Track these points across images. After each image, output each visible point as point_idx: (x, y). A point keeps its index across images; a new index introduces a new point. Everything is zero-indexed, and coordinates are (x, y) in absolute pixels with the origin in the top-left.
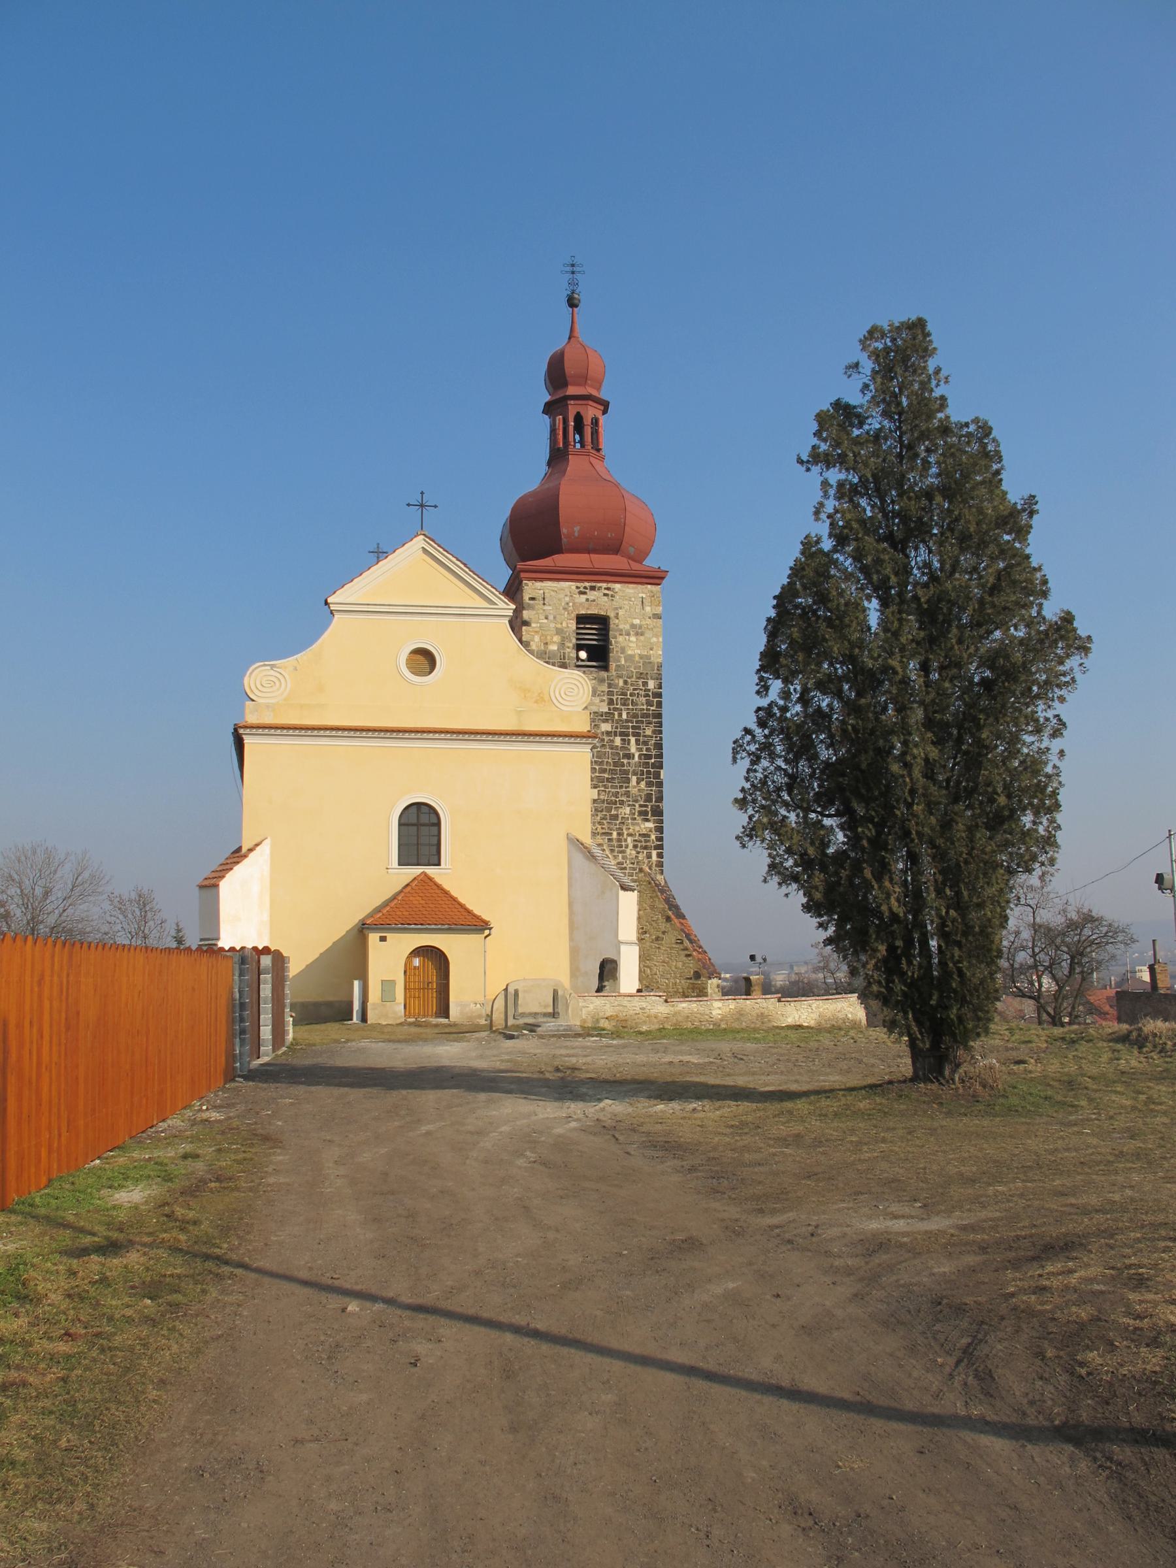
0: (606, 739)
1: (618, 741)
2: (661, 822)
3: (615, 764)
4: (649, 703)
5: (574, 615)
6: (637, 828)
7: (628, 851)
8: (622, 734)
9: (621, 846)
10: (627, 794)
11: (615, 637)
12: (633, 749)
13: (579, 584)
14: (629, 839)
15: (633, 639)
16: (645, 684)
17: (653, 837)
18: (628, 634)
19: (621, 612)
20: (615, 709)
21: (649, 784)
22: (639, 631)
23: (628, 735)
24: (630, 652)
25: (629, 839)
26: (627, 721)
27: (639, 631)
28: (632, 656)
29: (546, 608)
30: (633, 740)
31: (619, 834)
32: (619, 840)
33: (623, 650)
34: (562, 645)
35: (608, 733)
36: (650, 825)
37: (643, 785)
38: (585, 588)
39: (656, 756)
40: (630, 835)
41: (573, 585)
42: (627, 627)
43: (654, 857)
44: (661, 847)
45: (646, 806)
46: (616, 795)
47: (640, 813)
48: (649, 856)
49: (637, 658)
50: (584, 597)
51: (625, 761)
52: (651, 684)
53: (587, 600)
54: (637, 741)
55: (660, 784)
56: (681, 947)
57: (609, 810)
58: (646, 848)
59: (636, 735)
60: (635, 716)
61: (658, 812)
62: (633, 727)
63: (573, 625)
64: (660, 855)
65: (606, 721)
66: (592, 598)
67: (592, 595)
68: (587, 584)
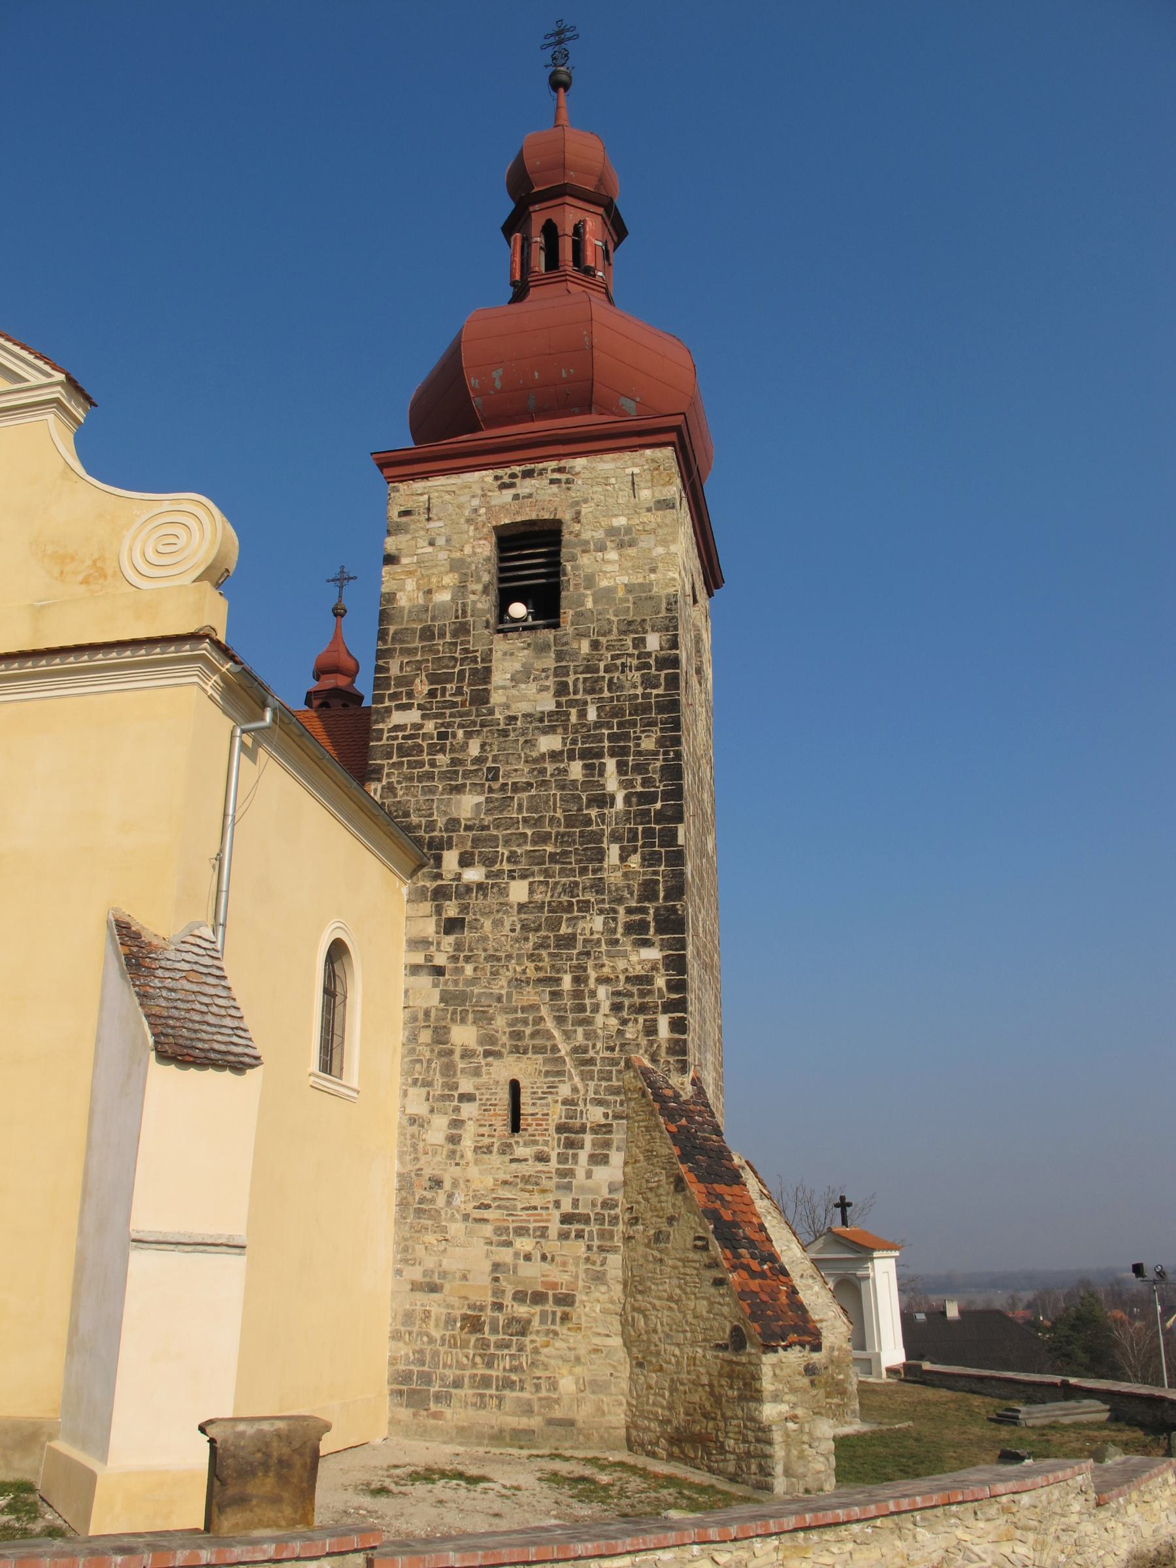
0: (550, 767)
1: (576, 770)
2: (682, 944)
3: (570, 821)
4: (648, 682)
6: (621, 964)
7: (599, 1020)
8: (585, 754)
9: (582, 1008)
10: (598, 886)
11: (573, 558)
12: (612, 783)
13: (500, 472)
14: (602, 992)
15: (612, 555)
16: (640, 642)
17: (660, 982)
18: (602, 548)
19: (585, 509)
20: (571, 704)
21: (650, 860)
22: (623, 539)
23: (600, 755)
24: (604, 583)
26: (598, 725)
27: (623, 539)
28: (610, 591)
29: (432, 525)
30: (611, 764)
31: (577, 980)
32: (577, 994)
33: (590, 581)
34: (461, 589)
35: (554, 756)
36: (653, 954)
37: (635, 861)
39: (667, 795)
40: (606, 980)
41: (488, 476)
42: (600, 534)
44: (680, 1005)
45: (644, 910)
46: (572, 889)
47: (629, 928)
48: (651, 1030)
49: (621, 593)
50: (508, 494)
51: (593, 812)
52: (653, 642)
53: (516, 497)
54: (621, 768)
55: (677, 858)
56: (702, 1257)
57: (554, 925)
58: (642, 1009)
59: (619, 752)
60: (617, 712)
61: (673, 924)
62: (612, 737)
63: (486, 549)
64: (678, 1026)
65: (551, 730)
66: (527, 491)
67: (525, 487)
68: (517, 469)
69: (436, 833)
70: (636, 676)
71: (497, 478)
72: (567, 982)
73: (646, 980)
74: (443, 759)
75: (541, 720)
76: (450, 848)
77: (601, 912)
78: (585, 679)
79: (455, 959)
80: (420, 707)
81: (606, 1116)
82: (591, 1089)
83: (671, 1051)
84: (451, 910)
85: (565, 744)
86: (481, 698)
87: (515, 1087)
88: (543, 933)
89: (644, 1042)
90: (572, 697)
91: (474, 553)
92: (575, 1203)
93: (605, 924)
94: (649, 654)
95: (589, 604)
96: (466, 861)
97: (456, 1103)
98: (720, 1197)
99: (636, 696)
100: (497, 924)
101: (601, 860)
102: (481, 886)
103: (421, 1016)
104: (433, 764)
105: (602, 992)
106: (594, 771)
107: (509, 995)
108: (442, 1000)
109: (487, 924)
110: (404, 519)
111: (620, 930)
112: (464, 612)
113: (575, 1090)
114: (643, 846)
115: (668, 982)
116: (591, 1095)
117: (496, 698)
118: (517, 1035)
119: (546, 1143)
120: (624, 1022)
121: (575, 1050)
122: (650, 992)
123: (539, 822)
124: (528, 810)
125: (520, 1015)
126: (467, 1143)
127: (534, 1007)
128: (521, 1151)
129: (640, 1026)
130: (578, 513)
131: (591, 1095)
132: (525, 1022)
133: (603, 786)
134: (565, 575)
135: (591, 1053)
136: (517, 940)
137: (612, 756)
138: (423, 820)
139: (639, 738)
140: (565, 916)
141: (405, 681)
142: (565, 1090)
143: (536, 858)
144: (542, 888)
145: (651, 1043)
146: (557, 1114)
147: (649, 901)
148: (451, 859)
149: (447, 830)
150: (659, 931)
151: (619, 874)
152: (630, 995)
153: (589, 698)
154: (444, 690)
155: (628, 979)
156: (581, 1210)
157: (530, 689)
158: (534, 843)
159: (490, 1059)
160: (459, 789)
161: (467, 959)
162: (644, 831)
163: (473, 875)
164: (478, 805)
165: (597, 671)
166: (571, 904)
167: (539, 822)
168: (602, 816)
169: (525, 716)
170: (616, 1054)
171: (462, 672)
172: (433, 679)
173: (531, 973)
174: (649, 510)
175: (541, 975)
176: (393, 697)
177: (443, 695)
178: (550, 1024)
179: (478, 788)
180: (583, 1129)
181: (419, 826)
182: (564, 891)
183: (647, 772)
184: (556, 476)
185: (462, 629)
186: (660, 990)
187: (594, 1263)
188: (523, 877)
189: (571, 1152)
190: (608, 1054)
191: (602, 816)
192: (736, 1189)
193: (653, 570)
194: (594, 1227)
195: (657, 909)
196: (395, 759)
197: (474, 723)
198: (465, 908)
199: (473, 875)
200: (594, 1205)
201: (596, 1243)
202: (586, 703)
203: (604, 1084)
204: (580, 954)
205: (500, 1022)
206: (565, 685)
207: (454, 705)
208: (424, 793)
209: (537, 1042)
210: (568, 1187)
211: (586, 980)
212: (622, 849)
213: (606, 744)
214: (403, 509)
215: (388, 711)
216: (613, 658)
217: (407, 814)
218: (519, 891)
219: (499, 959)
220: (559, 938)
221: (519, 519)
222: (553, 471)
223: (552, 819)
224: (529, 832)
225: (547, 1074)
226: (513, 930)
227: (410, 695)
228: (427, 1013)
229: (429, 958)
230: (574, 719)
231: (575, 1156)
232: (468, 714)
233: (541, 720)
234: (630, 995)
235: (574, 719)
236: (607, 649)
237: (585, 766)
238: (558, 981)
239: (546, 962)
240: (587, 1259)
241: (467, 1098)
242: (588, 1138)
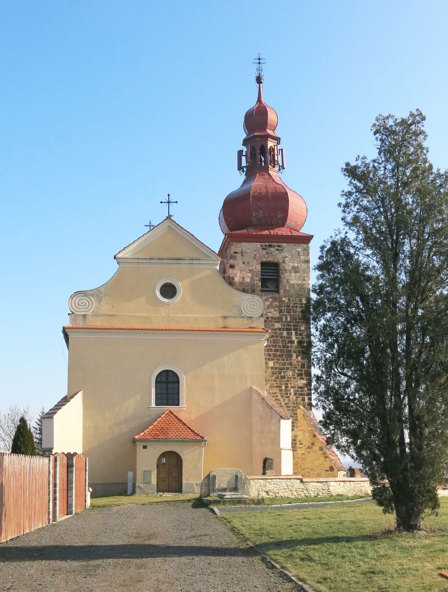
1: (285, 333)
3: (284, 347)
5: (259, 262)
7: (291, 397)
8: (287, 329)
9: (287, 394)
10: (291, 364)
13: (262, 244)
14: (292, 390)
15: (293, 274)
16: (301, 300)
20: (283, 315)
24: (292, 282)
25: (292, 390)
26: (290, 322)
28: (293, 285)
30: (293, 333)
31: (286, 387)
32: (286, 390)
33: (287, 281)
34: (252, 278)
35: (279, 329)
37: (300, 358)
38: (266, 246)
40: (293, 387)
41: (258, 245)
43: (307, 400)
45: (302, 371)
48: (303, 400)
49: (296, 286)
50: (265, 251)
51: (289, 345)
53: (267, 253)
54: (296, 334)
56: (322, 452)
57: (280, 373)
58: (301, 395)
59: (296, 330)
60: (295, 319)
62: (294, 325)
63: (259, 267)
65: (278, 322)
68: (267, 244)
71: (261, 246)
72: (283, 387)
77: (291, 370)
78: (287, 309)
88: (277, 375)
89: (302, 402)
93: (293, 373)
95: (288, 288)
101: (291, 357)
105: (292, 390)
106: (289, 334)
107: (269, 390)
110: (235, 254)
111: (296, 375)
112: (254, 285)
120: (297, 397)
121: (286, 404)
122: (303, 391)
123: (276, 346)
124: (273, 343)
129: (301, 399)
130: (284, 261)
134: (281, 278)
135: (289, 405)
136: (271, 376)
137: (294, 330)
140: (283, 371)
143: (275, 356)
144: (277, 364)
145: (304, 403)
151: (296, 361)
152: (298, 391)
155: (298, 387)
157: (272, 310)
158: (274, 352)
166: (284, 368)
167: (276, 346)
168: (291, 346)
169: (271, 317)
170: (295, 405)
173: (275, 385)
174: (303, 263)
175: (277, 385)
178: (279, 397)
182: (282, 365)
184: (278, 248)
188: (272, 360)
190: (293, 405)
191: (291, 346)
193: (304, 280)
195: (305, 370)
202: (287, 315)
203: (293, 412)
204: (286, 380)
206: (281, 310)
211: (288, 387)
212: (296, 355)
213: (292, 327)
214: (235, 251)
216: (294, 304)
220: (281, 376)
222: (277, 246)
223: (279, 346)
224: (273, 349)
230: (284, 320)
233: (275, 319)
234: (298, 391)
235: (284, 320)
236: (292, 301)
237: (287, 333)
238: (281, 387)
239: (279, 382)
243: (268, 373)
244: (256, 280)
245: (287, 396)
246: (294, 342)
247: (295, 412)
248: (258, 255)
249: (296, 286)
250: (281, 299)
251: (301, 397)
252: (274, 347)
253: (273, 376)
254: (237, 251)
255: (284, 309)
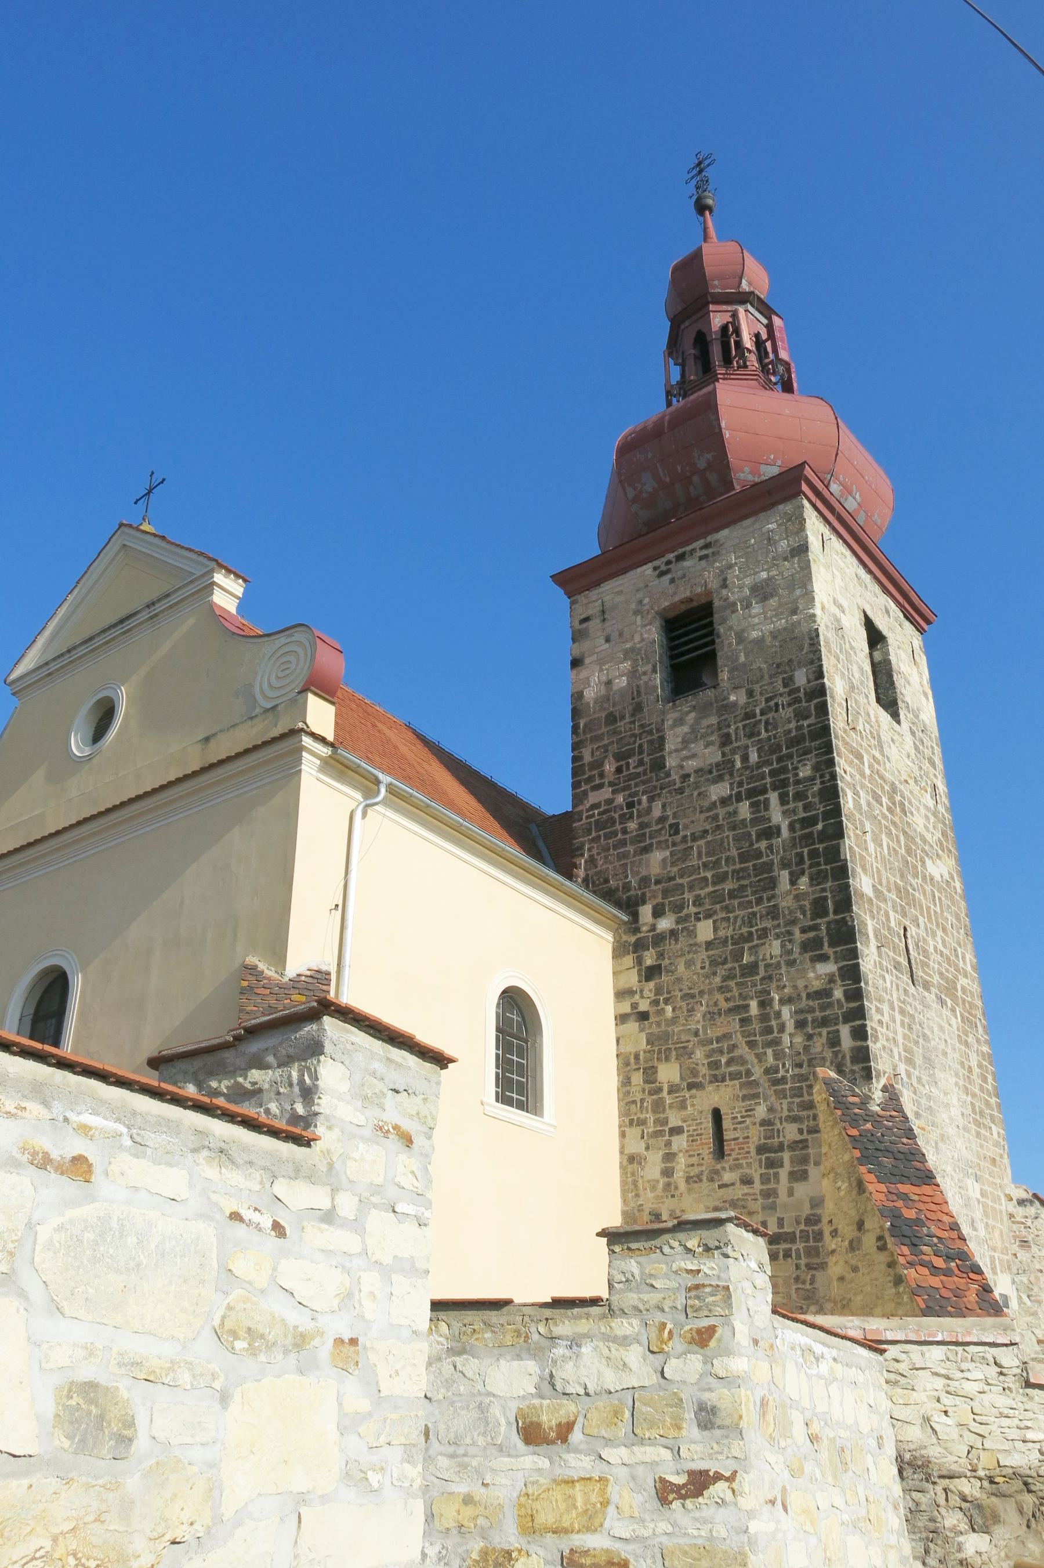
1: (744, 809)
3: (743, 858)
4: (801, 715)
7: (786, 1039)
8: (751, 794)
9: (769, 1030)
10: (773, 913)
13: (657, 563)
15: (756, 609)
16: (788, 681)
17: (838, 994)
21: (817, 879)
23: (763, 791)
24: (755, 634)
25: (786, 1012)
26: (759, 766)
28: (759, 642)
30: (773, 797)
31: (762, 1004)
32: (764, 1018)
33: (740, 638)
35: (724, 801)
38: (669, 563)
39: (827, 815)
41: (647, 570)
43: (847, 1042)
45: (815, 928)
47: (805, 947)
48: (834, 1041)
49: (768, 640)
51: (763, 845)
52: (801, 678)
54: (783, 800)
57: (738, 956)
58: (824, 1022)
59: (781, 785)
60: (776, 749)
62: (772, 773)
63: (654, 634)
65: (720, 778)
68: (671, 556)
69: (632, 893)
70: (787, 713)
71: (655, 569)
73: (826, 993)
74: (632, 825)
75: (710, 772)
76: (644, 903)
77: (777, 936)
79: (656, 1002)
80: (611, 784)
81: (801, 1131)
82: (785, 1107)
83: (855, 1060)
84: (649, 959)
85: (732, 789)
86: (658, 765)
87: (717, 1115)
88: (729, 965)
90: (735, 745)
91: (643, 640)
92: (781, 1222)
93: (783, 946)
94: (798, 689)
96: (658, 913)
97: (667, 1138)
98: (904, 1197)
99: (790, 731)
100: (689, 964)
102: (673, 933)
103: (632, 1061)
104: (625, 831)
105: (786, 1012)
106: (759, 807)
107: (705, 1028)
108: (648, 1043)
109: (681, 968)
110: (584, 625)
111: (797, 950)
112: (639, 692)
113: (771, 1110)
114: (811, 866)
115: (845, 992)
116: (785, 1113)
117: (671, 762)
118: (714, 1065)
119: (749, 1165)
120: (810, 1037)
121: (767, 1071)
122: (830, 1005)
123: (717, 863)
125: (715, 1045)
126: (679, 1176)
127: (726, 1036)
128: (727, 1177)
129: (824, 1040)
130: (725, 580)
131: (785, 1113)
132: (721, 1052)
133: (769, 820)
134: (719, 637)
135: (782, 1073)
137: (774, 790)
138: (620, 883)
139: (796, 768)
140: (746, 946)
141: (597, 764)
142: (761, 1111)
143: (717, 898)
144: (725, 924)
145: (836, 1054)
146: (756, 1135)
147: (821, 917)
148: (646, 912)
149: (640, 889)
150: (831, 945)
152: (811, 1010)
153: (749, 742)
154: (628, 764)
155: (808, 995)
156: (787, 1229)
157: (697, 747)
158: (714, 884)
159: (694, 1091)
160: (647, 850)
161: (667, 1001)
162: (810, 853)
163: (665, 924)
164: (664, 860)
165: (754, 716)
166: (750, 934)
167: (717, 863)
168: (770, 847)
169: (696, 772)
170: (804, 1070)
171: (641, 746)
172: (618, 757)
174: (786, 559)
175: (731, 1004)
176: (590, 779)
177: (628, 769)
178: (743, 1050)
179: (662, 845)
180: (781, 1148)
181: (617, 889)
183: (807, 797)
184: (704, 552)
185: (638, 708)
186: (839, 1001)
187: (804, 1283)
188: (708, 916)
189: (771, 1171)
190: (797, 1071)
191: (770, 847)
192: (926, 1189)
193: (794, 611)
194: (800, 1245)
196: (594, 834)
197: (655, 787)
198: (661, 955)
199: (665, 924)
200: (798, 1223)
201: (803, 1262)
202: (747, 747)
203: (797, 1100)
205: (699, 1054)
206: (727, 736)
207: (638, 775)
208: (619, 859)
209: (732, 1069)
210: (773, 1207)
212: (791, 874)
213: (768, 780)
214: (582, 617)
215: (585, 793)
216: (767, 700)
217: (606, 881)
218: (705, 930)
219: (693, 996)
221: (677, 599)
222: (701, 548)
225: (745, 1098)
226: (703, 968)
227: (602, 775)
228: (637, 1057)
229: (634, 1006)
230: (738, 764)
231: (776, 1175)
232: (649, 781)
233: (710, 772)
234: (811, 1010)
235: (738, 764)
240: (797, 1279)
241: (676, 1131)
242: (786, 1156)
243: (699, 965)
244: (645, 673)
245: (770, 1037)
246: (778, 828)
247: (806, 1098)
248: (646, 601)
249: (768, 640)
250: (726, 698)
251: (824, 1031)
252: (713, 868)
253: (715, 974)
254: (590, 612)
255: (737, 728)
